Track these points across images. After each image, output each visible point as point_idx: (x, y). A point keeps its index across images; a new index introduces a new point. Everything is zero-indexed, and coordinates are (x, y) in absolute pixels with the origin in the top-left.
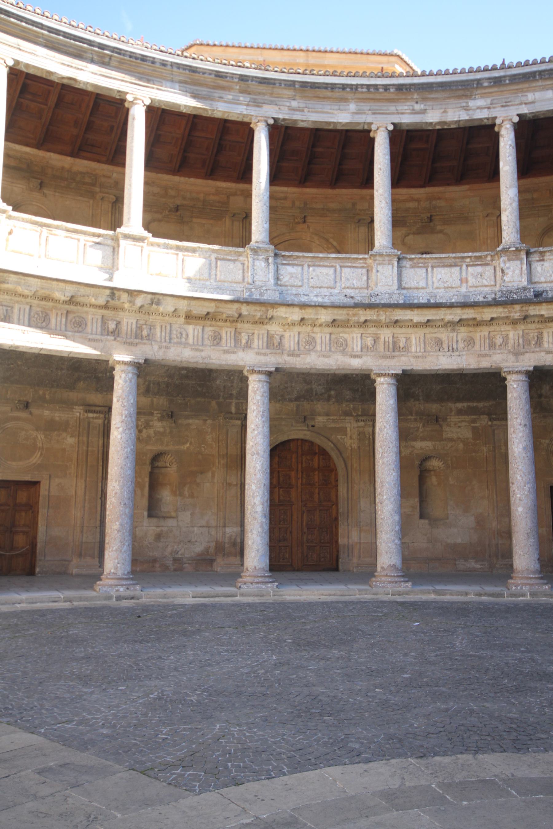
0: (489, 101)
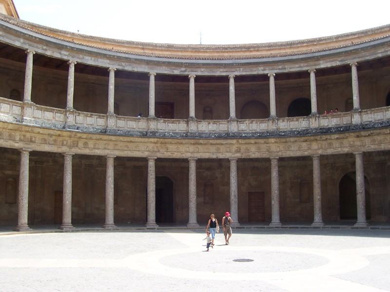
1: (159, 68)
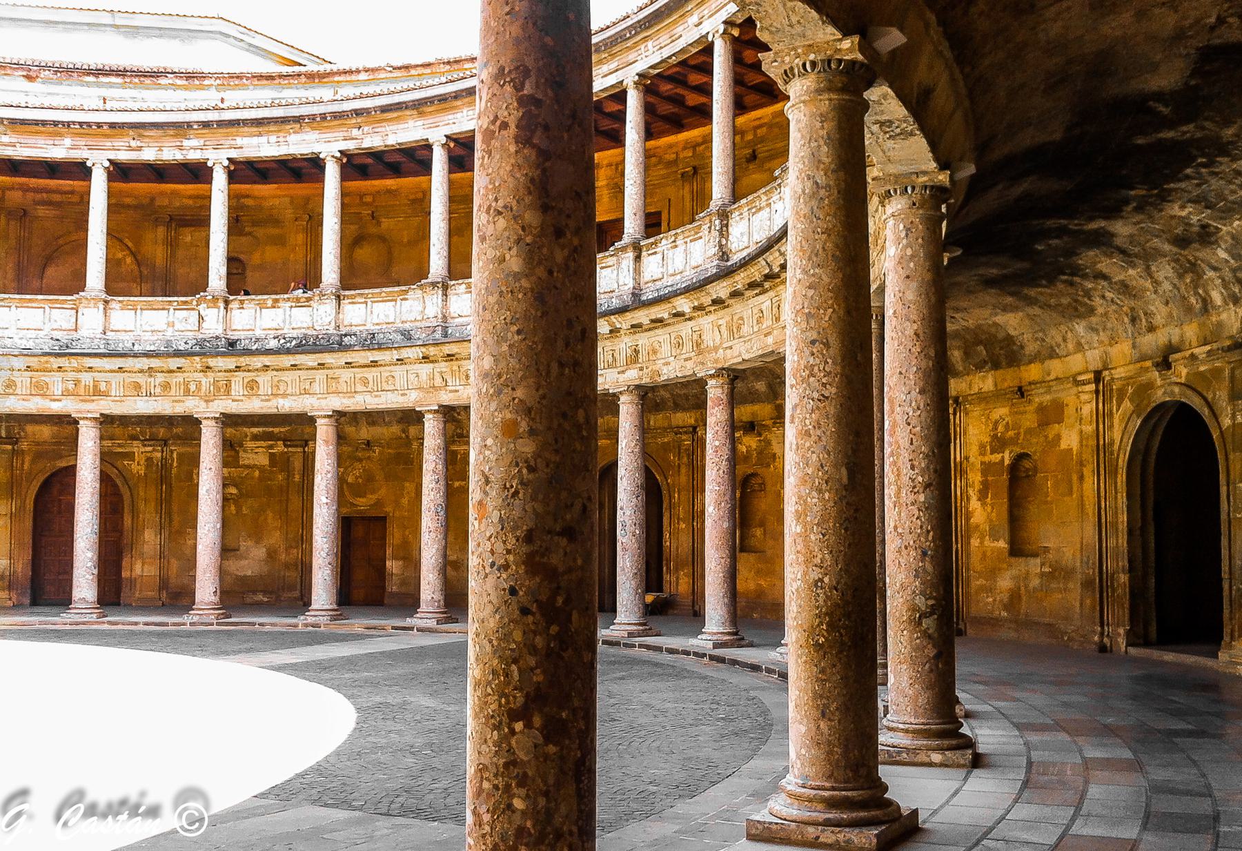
0: (202, 142)
1: (449, 117)
